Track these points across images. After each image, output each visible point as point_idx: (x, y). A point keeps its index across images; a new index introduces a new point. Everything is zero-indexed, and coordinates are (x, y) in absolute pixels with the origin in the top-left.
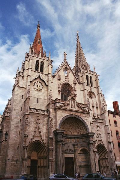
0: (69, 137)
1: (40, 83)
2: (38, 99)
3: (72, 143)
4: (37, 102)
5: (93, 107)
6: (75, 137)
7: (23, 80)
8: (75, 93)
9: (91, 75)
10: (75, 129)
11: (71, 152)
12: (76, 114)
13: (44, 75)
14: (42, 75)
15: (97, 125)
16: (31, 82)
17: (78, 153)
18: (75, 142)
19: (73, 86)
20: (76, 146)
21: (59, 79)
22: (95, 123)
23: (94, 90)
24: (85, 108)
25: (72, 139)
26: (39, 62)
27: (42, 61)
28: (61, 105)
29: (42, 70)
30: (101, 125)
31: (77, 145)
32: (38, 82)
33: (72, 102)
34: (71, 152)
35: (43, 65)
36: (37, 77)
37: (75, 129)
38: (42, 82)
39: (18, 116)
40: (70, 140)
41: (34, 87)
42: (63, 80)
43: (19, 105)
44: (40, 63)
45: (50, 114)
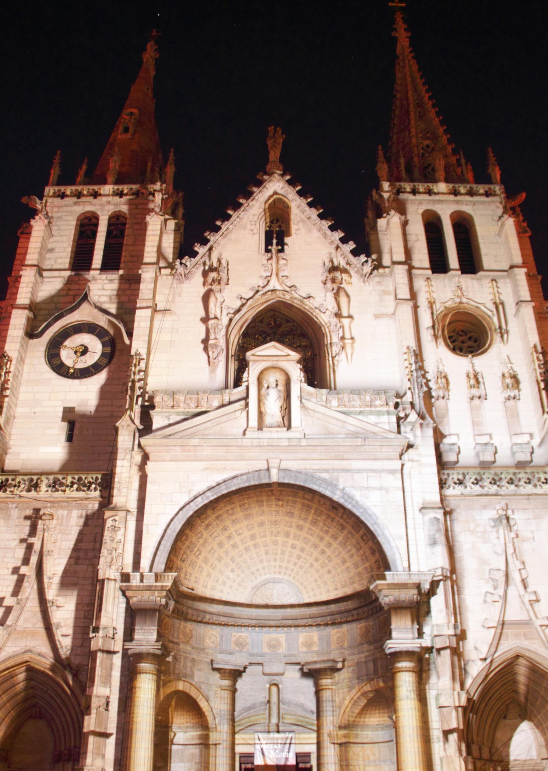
26: (96, 225)
35: (122, 232)
41: (56, 362)
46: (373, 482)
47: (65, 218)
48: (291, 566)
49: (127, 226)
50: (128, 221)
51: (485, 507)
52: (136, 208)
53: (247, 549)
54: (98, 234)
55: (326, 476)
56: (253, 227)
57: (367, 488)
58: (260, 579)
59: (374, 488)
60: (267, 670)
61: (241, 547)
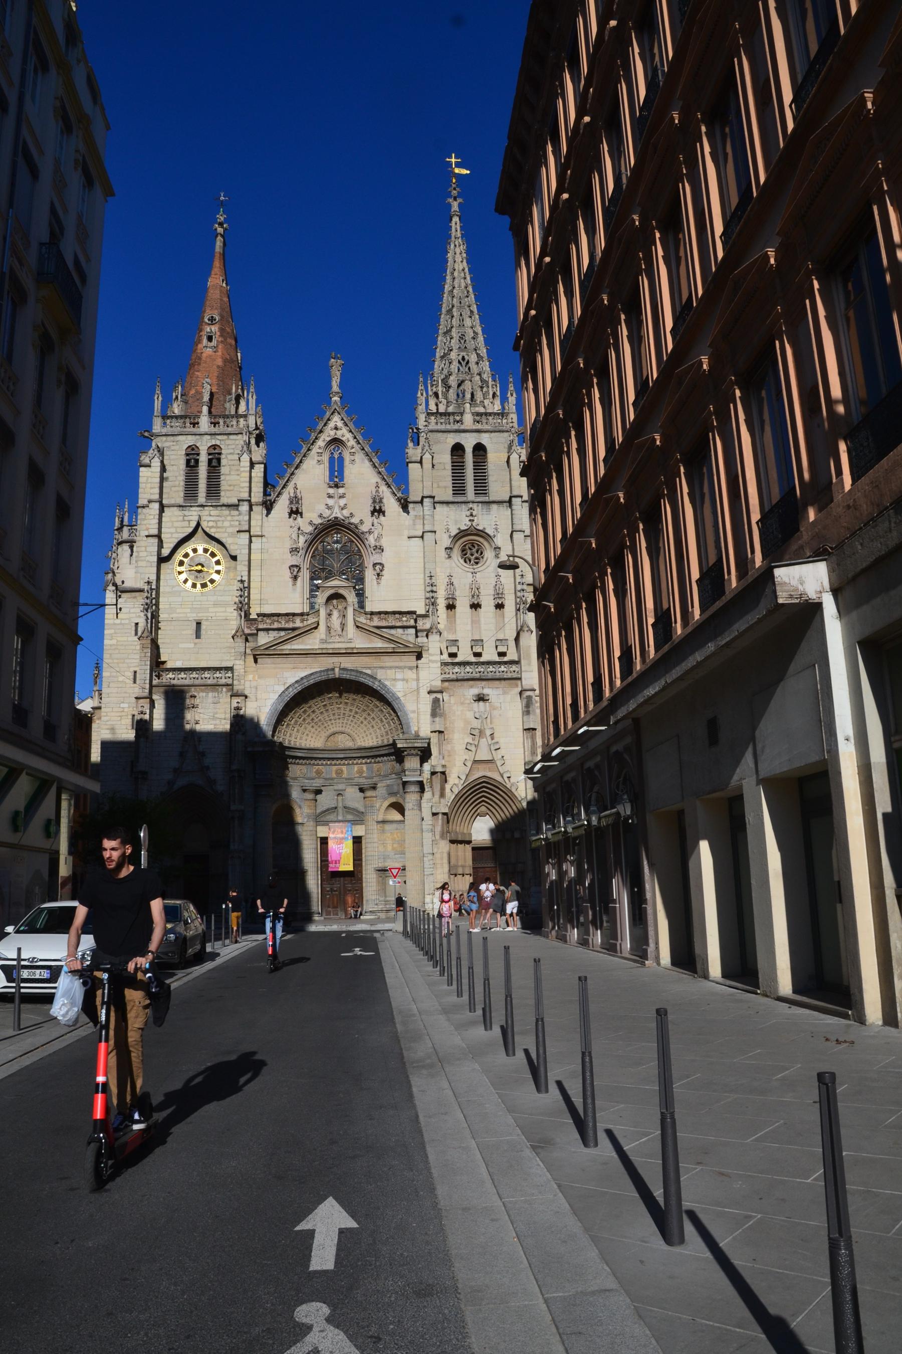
0: (342, 759)
1: (206, 551)
2: (199, 624)
3: (356, 780)
4: (198, 636)
5: (475, 606)
6: (363, 758)
7: (133, 561)
8: (376, 558)
9: (485, 439)
10: (365, 722)
11: (350, 817)
12: (348, 663)
13: (226, 512)
14: (212, 513)
15: (474, 690)
16: (162, 560)
17: (378, 822)
18: (366, 778)
19: (364, 528)
20: (369, 793)
21: (295, 512)
22: (466, 683)
23: (487, 520)
24: (393, 631)
25: (357, 764)
26: (198, 454)
27: (214, 447)
28: (278, 635)
29: (214, 489)
30: (500, 691)
31: (374, 788)
32: (195, 551)
33: (335, 613)
34: (350, 817)
35: (219, 460)
36: (190, 530)
37: (365, 722)
38: (213, 547)
39: (122, 705)
40: (344, 768)
42: (316, 509)
43: (125, 665)
44: (203, 459)
45: (235, 682)
46: (399, 676)
47: (173, 448)
48: (349, 722)
49: (223, 456)
50: (223, 452)
51: (472, 687)
52: (228, 439)
53: (322, 713)
54: (200, 464)
55: (369, 672)
56: (319, 458)
57: (395, 680)
58: (331, 731)
59: (399, 680)
60: (336, 787)
61: (318, 712)
